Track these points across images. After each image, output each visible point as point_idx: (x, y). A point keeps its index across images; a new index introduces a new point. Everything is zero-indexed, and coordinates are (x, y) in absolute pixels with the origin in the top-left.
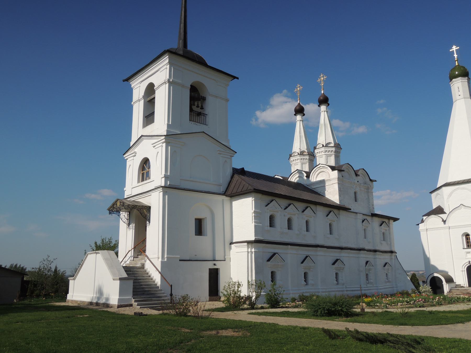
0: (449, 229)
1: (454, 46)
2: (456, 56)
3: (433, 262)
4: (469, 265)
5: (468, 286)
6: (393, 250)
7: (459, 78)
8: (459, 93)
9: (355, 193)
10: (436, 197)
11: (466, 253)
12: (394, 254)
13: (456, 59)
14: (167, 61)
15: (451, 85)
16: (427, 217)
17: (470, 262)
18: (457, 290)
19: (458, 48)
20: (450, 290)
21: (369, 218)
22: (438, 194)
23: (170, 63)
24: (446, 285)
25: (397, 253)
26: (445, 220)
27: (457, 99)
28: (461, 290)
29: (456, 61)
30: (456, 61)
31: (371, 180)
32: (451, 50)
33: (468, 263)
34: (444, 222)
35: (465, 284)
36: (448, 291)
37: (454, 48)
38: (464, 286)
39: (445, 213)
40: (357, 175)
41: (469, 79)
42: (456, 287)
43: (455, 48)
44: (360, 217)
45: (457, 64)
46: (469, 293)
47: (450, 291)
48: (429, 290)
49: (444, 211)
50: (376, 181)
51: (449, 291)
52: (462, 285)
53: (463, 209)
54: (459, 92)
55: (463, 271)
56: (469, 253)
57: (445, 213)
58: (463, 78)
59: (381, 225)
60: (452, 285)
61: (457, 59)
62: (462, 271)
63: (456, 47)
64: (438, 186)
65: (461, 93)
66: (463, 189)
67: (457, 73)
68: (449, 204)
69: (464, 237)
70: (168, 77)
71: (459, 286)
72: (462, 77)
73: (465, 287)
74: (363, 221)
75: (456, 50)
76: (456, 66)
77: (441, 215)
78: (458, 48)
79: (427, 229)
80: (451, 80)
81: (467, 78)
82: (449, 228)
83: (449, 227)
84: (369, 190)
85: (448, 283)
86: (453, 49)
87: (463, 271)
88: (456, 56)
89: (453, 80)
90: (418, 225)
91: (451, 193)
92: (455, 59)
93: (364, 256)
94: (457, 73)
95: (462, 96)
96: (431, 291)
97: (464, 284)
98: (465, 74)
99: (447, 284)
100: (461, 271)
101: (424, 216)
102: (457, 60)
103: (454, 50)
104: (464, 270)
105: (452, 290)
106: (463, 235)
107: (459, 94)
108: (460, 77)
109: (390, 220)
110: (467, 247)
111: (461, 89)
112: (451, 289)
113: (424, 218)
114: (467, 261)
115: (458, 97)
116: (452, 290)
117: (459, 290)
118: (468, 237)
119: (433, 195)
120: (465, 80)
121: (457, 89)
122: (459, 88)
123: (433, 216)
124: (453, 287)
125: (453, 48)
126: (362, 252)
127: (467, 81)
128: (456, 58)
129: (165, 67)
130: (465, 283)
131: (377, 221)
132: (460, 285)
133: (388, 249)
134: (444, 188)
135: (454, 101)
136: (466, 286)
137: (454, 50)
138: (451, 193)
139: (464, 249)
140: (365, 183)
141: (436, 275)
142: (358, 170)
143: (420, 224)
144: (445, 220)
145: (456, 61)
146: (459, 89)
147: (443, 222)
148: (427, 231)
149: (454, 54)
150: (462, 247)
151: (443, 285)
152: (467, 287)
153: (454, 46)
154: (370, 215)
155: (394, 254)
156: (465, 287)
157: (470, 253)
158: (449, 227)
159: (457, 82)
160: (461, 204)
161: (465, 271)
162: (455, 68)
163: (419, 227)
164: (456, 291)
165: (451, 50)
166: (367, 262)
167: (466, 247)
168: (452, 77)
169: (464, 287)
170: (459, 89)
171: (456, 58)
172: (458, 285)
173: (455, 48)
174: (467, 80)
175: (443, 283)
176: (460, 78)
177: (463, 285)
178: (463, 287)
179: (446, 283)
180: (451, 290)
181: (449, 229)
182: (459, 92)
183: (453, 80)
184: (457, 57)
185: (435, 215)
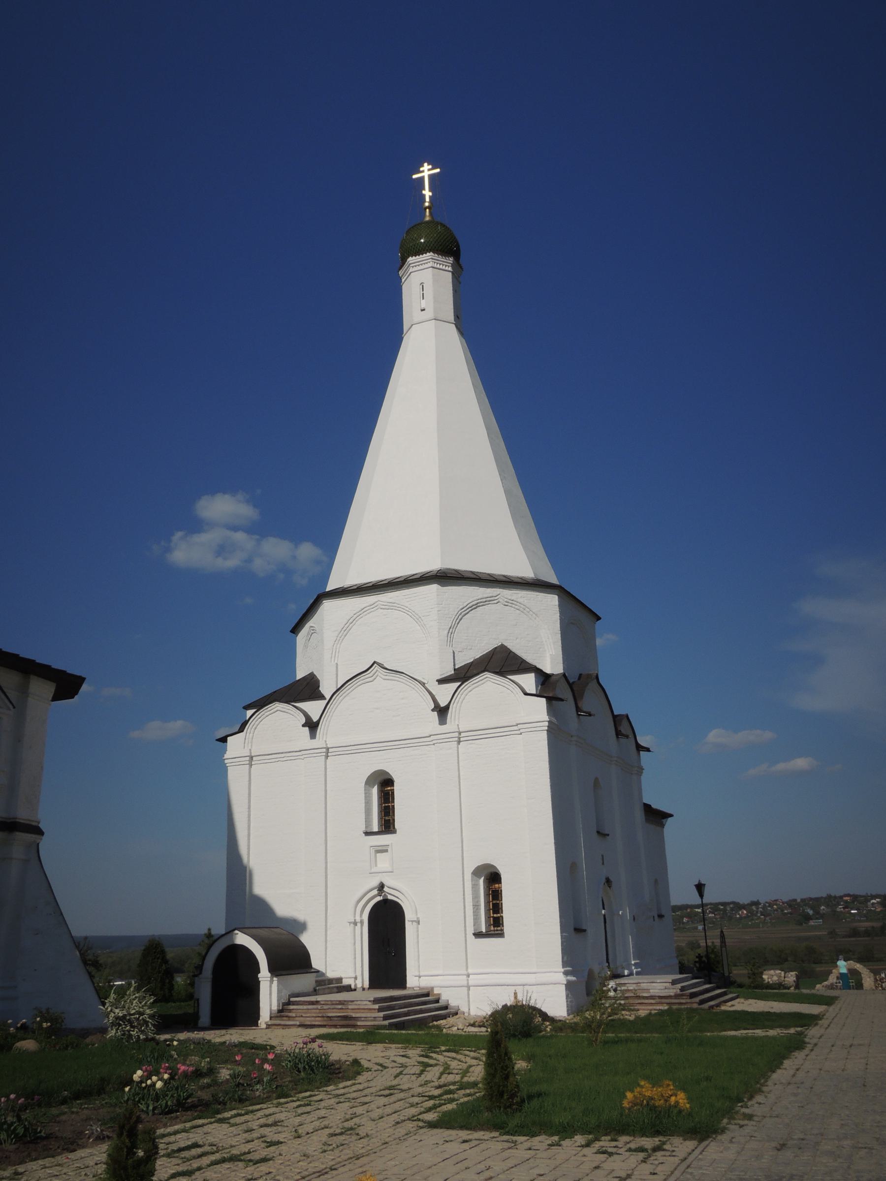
0: (327, 757)
1: (426, 164)
2: (427, 193)
3: (261, 887)
4: (379, 899)
5: (367, 984)
6: (23, 815)
7: (428, 254)
8: (423, 302)
10: (306, 646)
11: (373, 851)
12: (17, 833)
13: (427, 204)
15: (403, 280)
16: (254, 710)
17: (381, 887)
18: (312, 1003)
19: (438, 170)
20: (284, 1004)
22: (313, 631)
24: (271, 982)
25: (40, 832)
26: (315, 719)
27: (416, 320)
28: (326, 1003)
29: (428, 210)
30: (426, 208)
32: (414, 176)
33: (375, 892)
34: (312, 726)
35: (356, 978)
36: (275, 1007)
37: (426, 171)
38: (353, 987)
39: (322, 697)
42: (315, 990)
43: (429, 170)
46: (351, 1018)
47: (282, 1011)
48: (141, 1014)
49: (320, 689)
51: (280, 1011)
52: (345, 982)
53: (379, 682)
54: (423, 299)
55: (355, 923)
56: (382, 850)
57: (322, 697)
58: (440, 258)
60: (302, 982)
61: (431, 201)
62: (352, 925)
63: (430, 167)
66: (391, 606)
67: (422, 241)
68: (337, 664)
69: (375, 790)
71: (326, 984)
72: (438, 254)
73: (355, 990)
75: (430, 176)
77: (306, 706)
78: (438, 170)
79: (251, 758)
82: (328, 752)
83: (328, 749)
85: (276, 976)
86: (423, 171)
87: (355, 923)
88: (427, 193)
89: (411, 259)
90: (224, 740)
91: (351, 622)
92: (425, 201)
94: (422, 241)
95: (429, 313)
96: (152, 1016)
97: (354, 976)
99: (275, 979)
100: (350, 923)
101: (247, 708)
102: (429, 207)
103: (422, 178)
104: (358, 919)
105: (294, 1003)
106: (370, 782)
107: (423, 306)
108: (431, 254)
109: (32, 677)
110: (380, 825)
111: (429, 291)
112: (292, 999)
113: (249, 713)
114: (375, 883)
115: (418, 316)
116: (294, 1003)
117: (317, 1002)
118: (389, 788)
121: (417, 289)
122: (423, 286)
123: (278, 706)
124: (297, 990)
125: (421, 169)
127: (450, 269)
128: (427, 199)
130: (359, 974)
132: (340, 980)
135: (406, 327)
136: (359, 985)
137: (423, 178)
138: (351, 622)
139: (367, 834)
141: (242, 939)
143: (229, 738)
144: (315, 719)
145: (428, 210)
146: (423, 290)
147: (307, 729)
148: (251, 765)
149: (424, 189)
150: (363, 829)
151: (257, 983)
152: (364, 989)
153: (426, 164)
155: (20, 836)
156: (355, 990)
157: (386, 851)
158: (328, 749)
159: (418, 268)
160: (375, 662)
161: (362, 922)
163: (225, 750)
164: (305, 1007)
165: (414, 176)
167: (376, 829)
169: (352, 990)
170: (423, 290)
171: (427, 199)
172: (331, 981)
173: (429, 170)
174: (453, 266)
175: (259, 975)
176: (429, 255)
177: (351, 982)
178: (348, 988)
179: (269, 975)
180: (289, 1003)
181: (327, 757)
182: (423, 299)
183: (408, 260)
184: (430, 197)
185: (288, 702)
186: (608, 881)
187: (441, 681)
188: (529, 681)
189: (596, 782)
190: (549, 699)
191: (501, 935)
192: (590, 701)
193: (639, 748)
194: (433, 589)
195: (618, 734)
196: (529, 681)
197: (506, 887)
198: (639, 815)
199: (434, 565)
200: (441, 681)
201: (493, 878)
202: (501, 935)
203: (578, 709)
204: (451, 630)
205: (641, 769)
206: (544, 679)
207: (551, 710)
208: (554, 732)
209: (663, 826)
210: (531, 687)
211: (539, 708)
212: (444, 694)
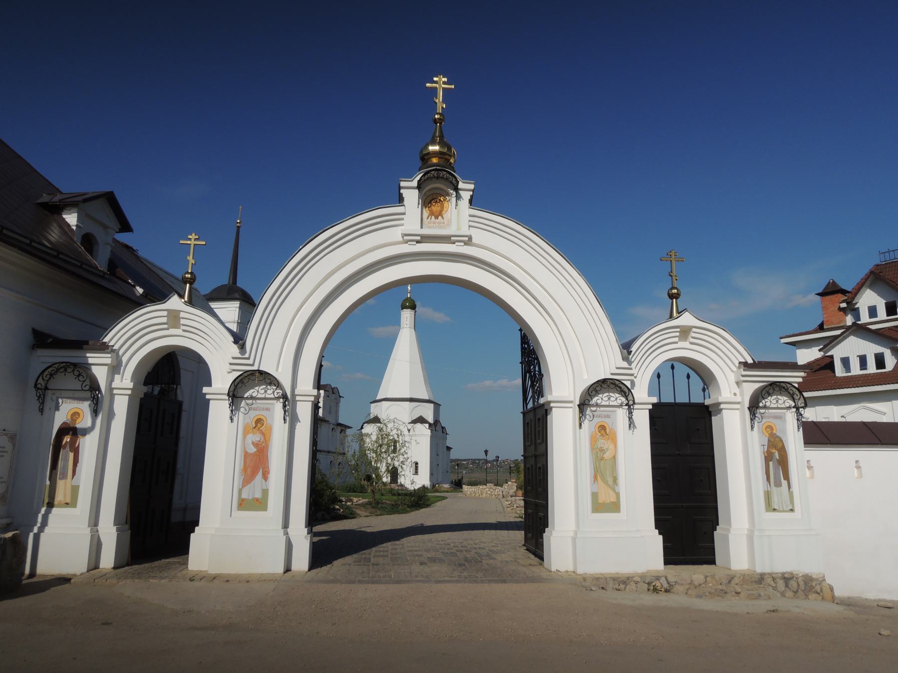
9: (330, 407)
14: (238, 305)
21: (335, 427)
22: (377, 406)
23: (240, 308)
31: (340, 397)
40: (333, 393)
41: (415, 312)
44: (331, 426)
45: (409, 296)
50: (343, 397)
59: (341, 433)
64: (378, 398)
65: (408, 322)
70: (237, 319)
74: (332, 430)
76: (408, 298)
80: (402, 309)
81: (414, 311)
84: (338, 403)
89: (404, 310)
91: (389, 407)
93: (331, 457)
95: (408, 326)
98: (413, 307)
111: (408, 319)
113: (366, 424)
119: (373, 405)
120: (412, 312)
126: (330, 454)
129: (234, 309)
131: (339, 429)
133: (342, 451)
134: (383, 402)
138: (389, 407)
140: (336, 399)
142: (334, 388)
154: (336, 424)
162: (407, 299)
166: (331, 462)
168: (404, 307)
176: (409, 310)
186: (438, 465)
187: (409, 423)
188: (427, 425)
189: (437, 444)
190: (431, 430)
191: (418, 475)
192: (439, 428)
193: (447, 434)
194: (408, 403)
195: (443, 432)
196: (427, 425)
197: (419, 465)
198: (445, 448)
199: (408, 396)
200: (409, 423)
201: (417, 464)
202: (418, 475)
203: (436, 430)
204: (411, 413)
205: (446, 439)
206: (430, 425)
207: (431, 433)
208: (431, 437)
209: (450, 451)
210: (428, 428)
211: (429, 432)
212: (410, 426)
